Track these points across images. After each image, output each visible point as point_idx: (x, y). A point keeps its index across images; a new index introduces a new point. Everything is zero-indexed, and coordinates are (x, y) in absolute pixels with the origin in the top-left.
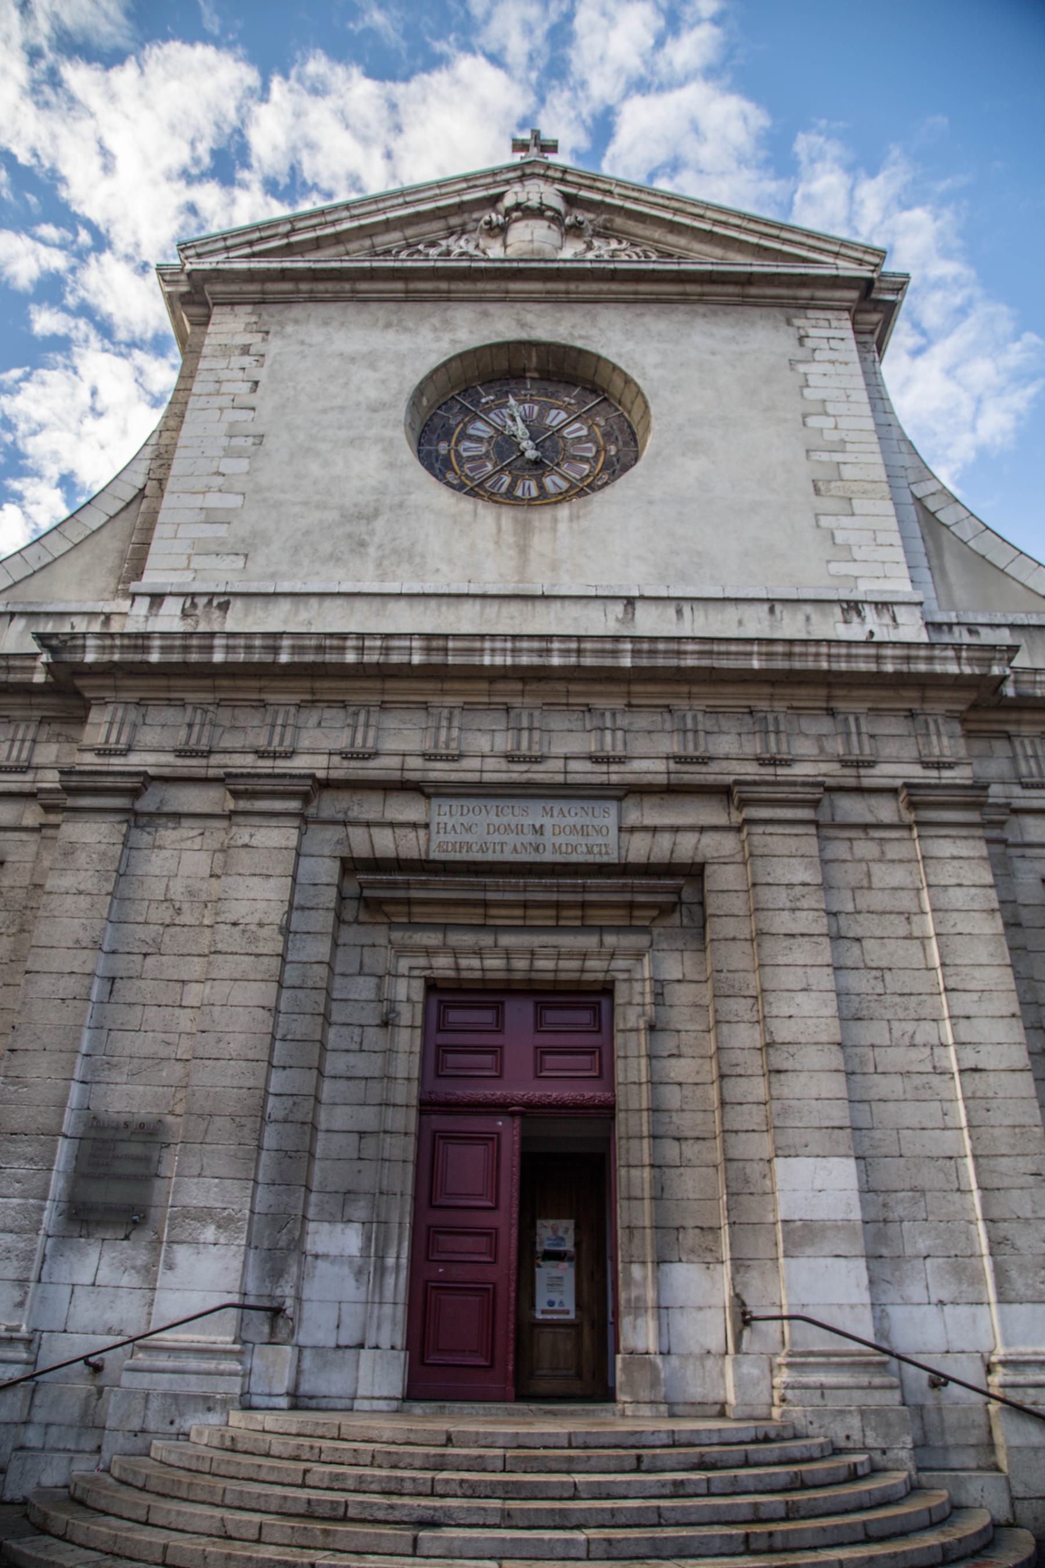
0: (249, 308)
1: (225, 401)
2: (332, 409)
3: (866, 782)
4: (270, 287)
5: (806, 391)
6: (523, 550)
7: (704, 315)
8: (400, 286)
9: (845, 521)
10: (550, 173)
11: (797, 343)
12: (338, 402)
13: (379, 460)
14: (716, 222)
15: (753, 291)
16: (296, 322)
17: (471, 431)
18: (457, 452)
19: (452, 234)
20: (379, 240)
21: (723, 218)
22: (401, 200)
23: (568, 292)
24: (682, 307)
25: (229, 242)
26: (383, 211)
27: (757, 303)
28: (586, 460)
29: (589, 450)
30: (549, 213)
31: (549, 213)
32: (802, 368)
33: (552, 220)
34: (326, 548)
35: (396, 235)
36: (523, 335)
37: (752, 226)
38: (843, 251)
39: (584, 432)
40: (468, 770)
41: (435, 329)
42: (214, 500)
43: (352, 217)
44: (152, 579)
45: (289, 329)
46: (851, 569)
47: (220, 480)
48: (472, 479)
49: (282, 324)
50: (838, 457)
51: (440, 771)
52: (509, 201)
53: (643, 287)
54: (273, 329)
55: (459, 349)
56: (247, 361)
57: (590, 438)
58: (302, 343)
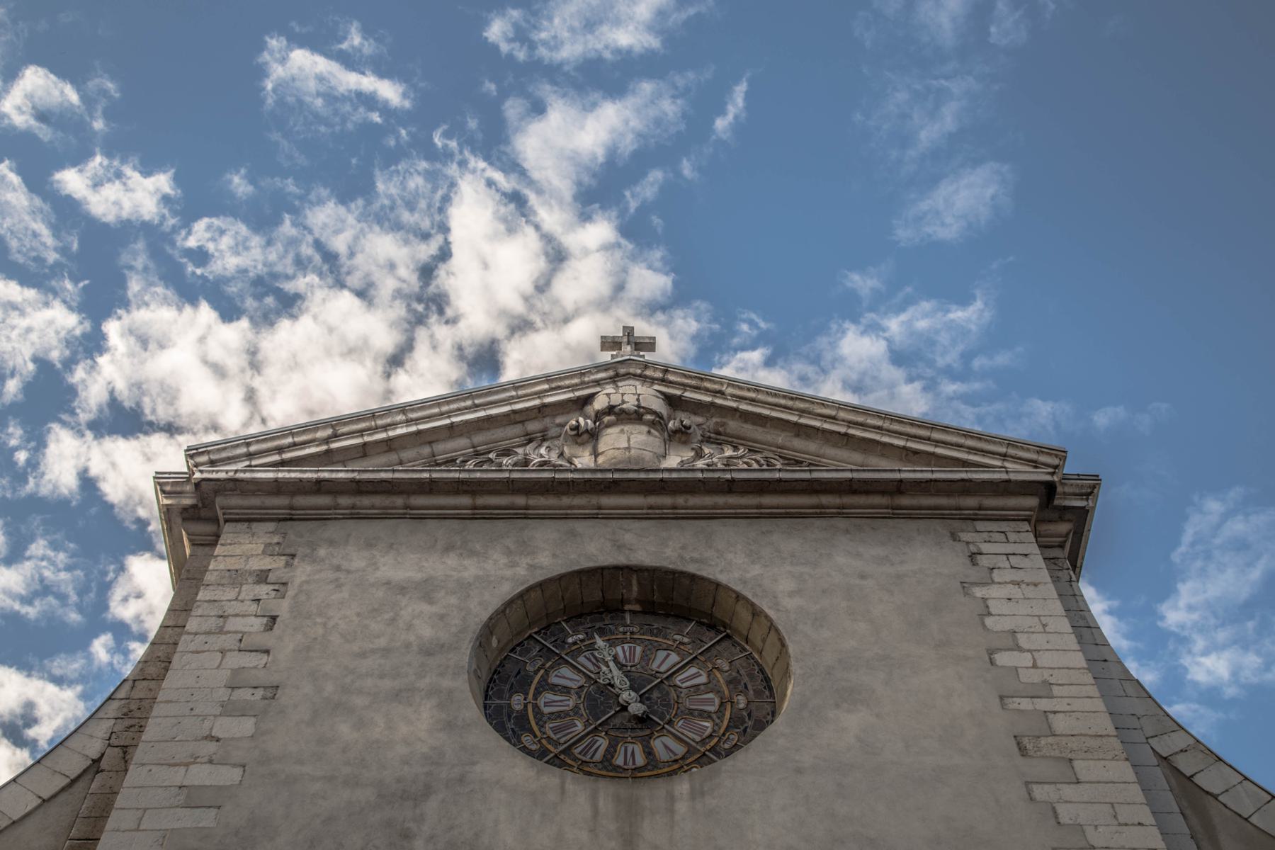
0: (271, 526)
1: (229, 641)
2: (373, 651)
4: (301, 501)
5: (989, 621)
7: (847, 531)
8: (465, 500)
9: (1068, 791)
10: (648, 373)
11: (968, 561)
12: (382, 642)
15: (905, 501)
16: (332, 543)
17: (553, 680)
18: (536, 706)
19: (530, 441)
20: (439, 447)
21: (860, 419)
22: (469, 403)
23: (675, 508)
24: (818, 522)
25: (253, 448)
26: (448, 414)
27: (912, 515)
28: (706, 715)
29: (711, 701)
30: (649, 417)
31: (649, 417)
32: (979, 592)
33: (652, 424)
35: (462, 442)
36: (621, 560)
37: (896, 427)
38: (1011, 451)
39: (703, 679)
41: (509, 552)
42: (200, 775)
43: (409, 422)
45: (322, 552)
47: (212, 747)
48: (557, 743)
49: (313, 546)
50: (1043, 704)
52: (600, 403)
53: (768, 500)
54: (301, 551)
55: (540, 576)
56: (263, 590)
57: (710, 686)
58: (338, 568)
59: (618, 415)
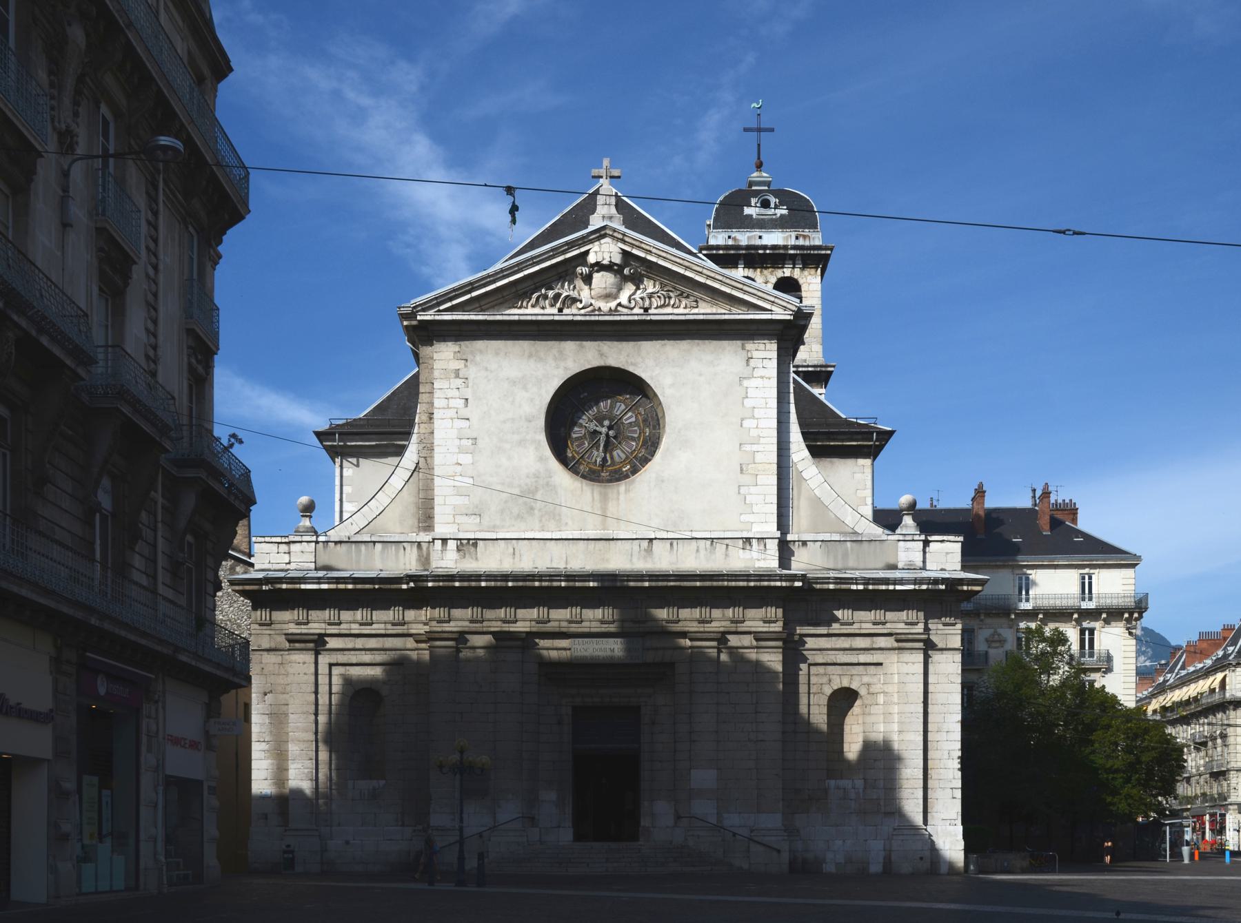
1: (452, 413)
3: (740, 629)
5: (746, 401)
9: (753, 489)
14: (708, 277)
16: (481, 352)
21: (712, 275)
28: (633, 439)
32: (746, 383)
34: (515, 511)
39: (633, 419)
40: (585, 627)
41: (555, 359)
44: (441, 529)
45: (478, 358)
46: (751, 518)
47: (459, 468)
48: (578, 453)
49: (472, 353)
50: (755, 448)
51: (574, 628)
52: (592, 259)
54: (470, 357)
56: (459, 382)
57: (636, 423)
58: (486, 369)
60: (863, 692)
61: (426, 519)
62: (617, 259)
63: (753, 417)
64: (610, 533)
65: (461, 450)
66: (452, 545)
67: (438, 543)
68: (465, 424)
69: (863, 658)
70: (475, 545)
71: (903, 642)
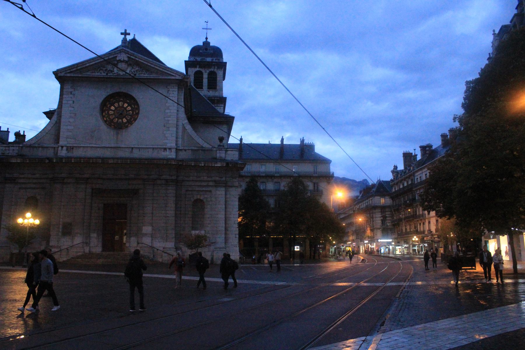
6: (117, 138)
9: (168, 132)
13: (95, 120)
42: (69, 127)
44: (61, 143)
46: (166, 141)
52: (118, 59)
56: (71, 96)
59: (120, 61)
60: (205, 201)
61: (57, 140)
62: (126, 59)
63: (169, 109)
64: (118, 145)
65: (71, 117)
66: (65, 148)
67: (60, 148)
68: (73, 109)
69: (204, 189)
70: (73, 148)
71: (217, 184)
